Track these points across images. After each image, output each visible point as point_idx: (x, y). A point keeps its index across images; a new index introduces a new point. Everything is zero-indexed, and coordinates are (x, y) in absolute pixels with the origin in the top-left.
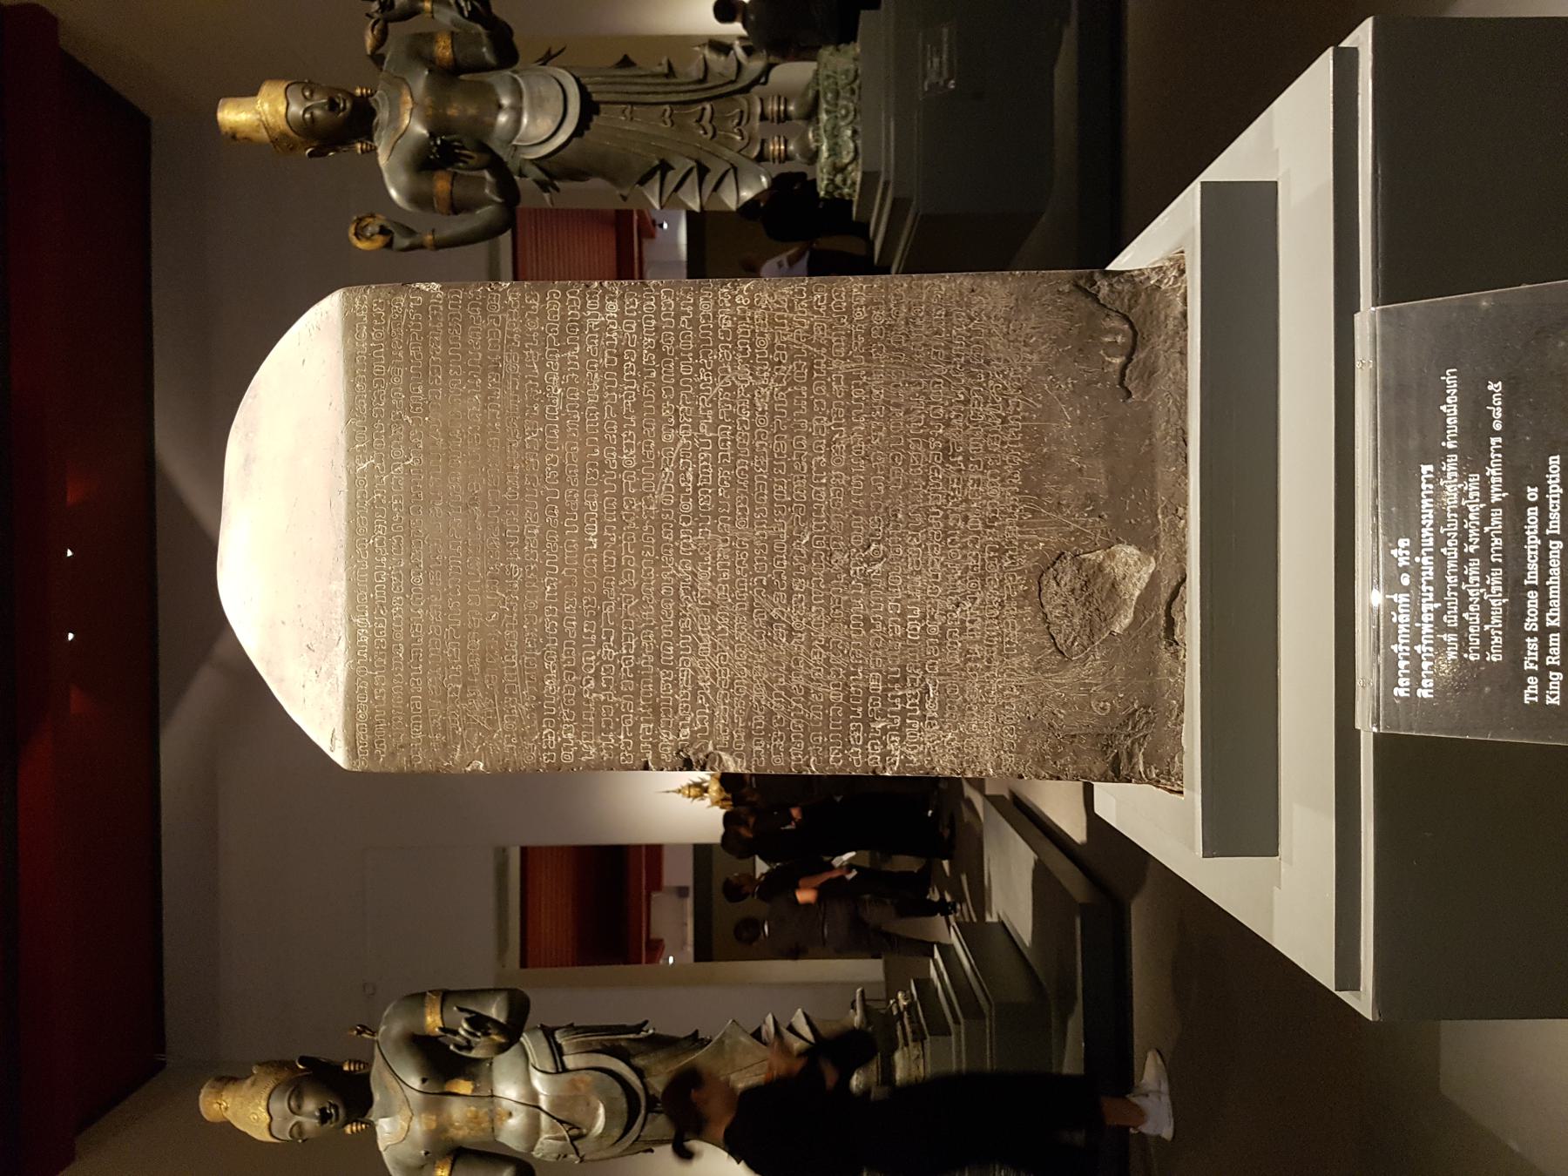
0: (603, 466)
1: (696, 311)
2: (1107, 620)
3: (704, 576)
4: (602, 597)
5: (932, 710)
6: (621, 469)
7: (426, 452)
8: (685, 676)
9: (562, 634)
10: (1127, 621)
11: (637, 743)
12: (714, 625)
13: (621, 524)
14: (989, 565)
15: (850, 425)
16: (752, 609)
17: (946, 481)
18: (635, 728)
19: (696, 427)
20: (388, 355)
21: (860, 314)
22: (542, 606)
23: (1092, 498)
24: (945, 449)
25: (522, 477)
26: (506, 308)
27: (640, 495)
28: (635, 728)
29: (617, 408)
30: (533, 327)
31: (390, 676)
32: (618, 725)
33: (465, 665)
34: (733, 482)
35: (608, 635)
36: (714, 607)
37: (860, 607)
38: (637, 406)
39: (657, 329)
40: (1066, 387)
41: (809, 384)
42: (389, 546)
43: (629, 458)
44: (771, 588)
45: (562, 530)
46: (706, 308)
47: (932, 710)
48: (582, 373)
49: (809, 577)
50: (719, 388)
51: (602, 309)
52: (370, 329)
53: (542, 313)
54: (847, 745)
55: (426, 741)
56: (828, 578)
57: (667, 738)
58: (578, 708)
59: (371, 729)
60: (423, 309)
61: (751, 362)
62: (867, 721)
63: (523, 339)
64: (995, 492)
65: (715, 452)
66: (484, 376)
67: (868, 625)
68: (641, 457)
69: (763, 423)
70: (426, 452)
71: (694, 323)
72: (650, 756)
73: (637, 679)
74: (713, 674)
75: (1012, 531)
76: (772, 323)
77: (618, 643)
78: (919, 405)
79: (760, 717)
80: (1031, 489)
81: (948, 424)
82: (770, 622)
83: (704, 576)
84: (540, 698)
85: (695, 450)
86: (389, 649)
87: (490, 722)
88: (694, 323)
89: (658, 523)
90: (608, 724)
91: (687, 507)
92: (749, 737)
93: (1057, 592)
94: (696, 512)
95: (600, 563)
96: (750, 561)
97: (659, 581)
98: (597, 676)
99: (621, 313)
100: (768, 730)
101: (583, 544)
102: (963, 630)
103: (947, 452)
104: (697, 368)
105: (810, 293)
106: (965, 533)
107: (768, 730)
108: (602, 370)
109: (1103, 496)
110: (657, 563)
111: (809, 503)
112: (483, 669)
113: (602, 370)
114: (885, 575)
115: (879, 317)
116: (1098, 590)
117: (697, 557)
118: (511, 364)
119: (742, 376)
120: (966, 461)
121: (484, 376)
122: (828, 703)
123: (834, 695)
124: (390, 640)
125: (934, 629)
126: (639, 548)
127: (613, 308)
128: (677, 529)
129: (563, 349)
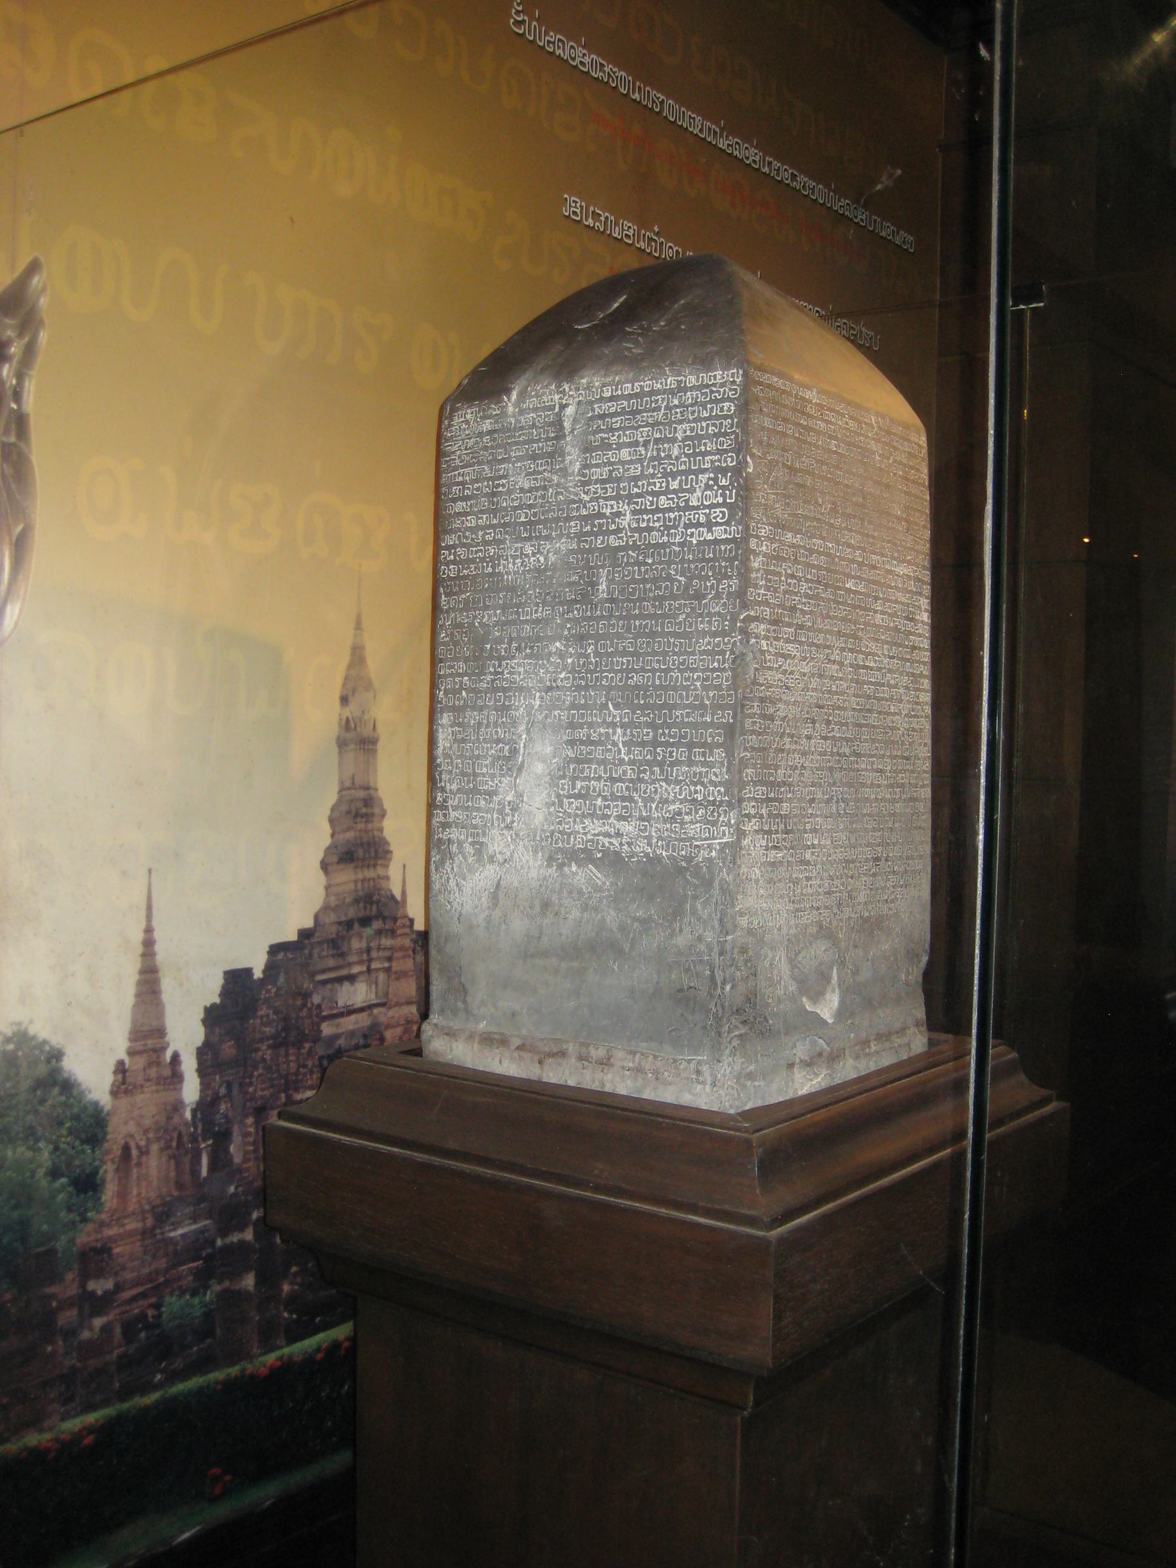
0: (876, 598)
8: (791, 648)
11: (759, 604)
12: (813, 675)
13: (855, 607)
16: (820, 707)
18: (766, 603)
22: (822, 538)
25: (873, 537)
28: (766, 603)
33: (800, 470)
34: (869, 697)
35: (810, 588)
42: (846, 429)
54: (755, 783)
55: (763, 429)
63: (917, 551)
67: (812, 800)
72: (752, 613)
74: (792, 673)
77: (807, 596)
82: (814, 722)
84: (784, 527)
86: (803, 413)
87: (772, 483)
89: (855, 637)
90: (770, 581)
92: (762, 700)
95: (840, 589)
96: (839, 708)
98: (793, 576)
100: (764, 716)
112: (798, 485)
120: (874, 875)
121: (907, 521)
122: (777, 767)
124: (809, 416)
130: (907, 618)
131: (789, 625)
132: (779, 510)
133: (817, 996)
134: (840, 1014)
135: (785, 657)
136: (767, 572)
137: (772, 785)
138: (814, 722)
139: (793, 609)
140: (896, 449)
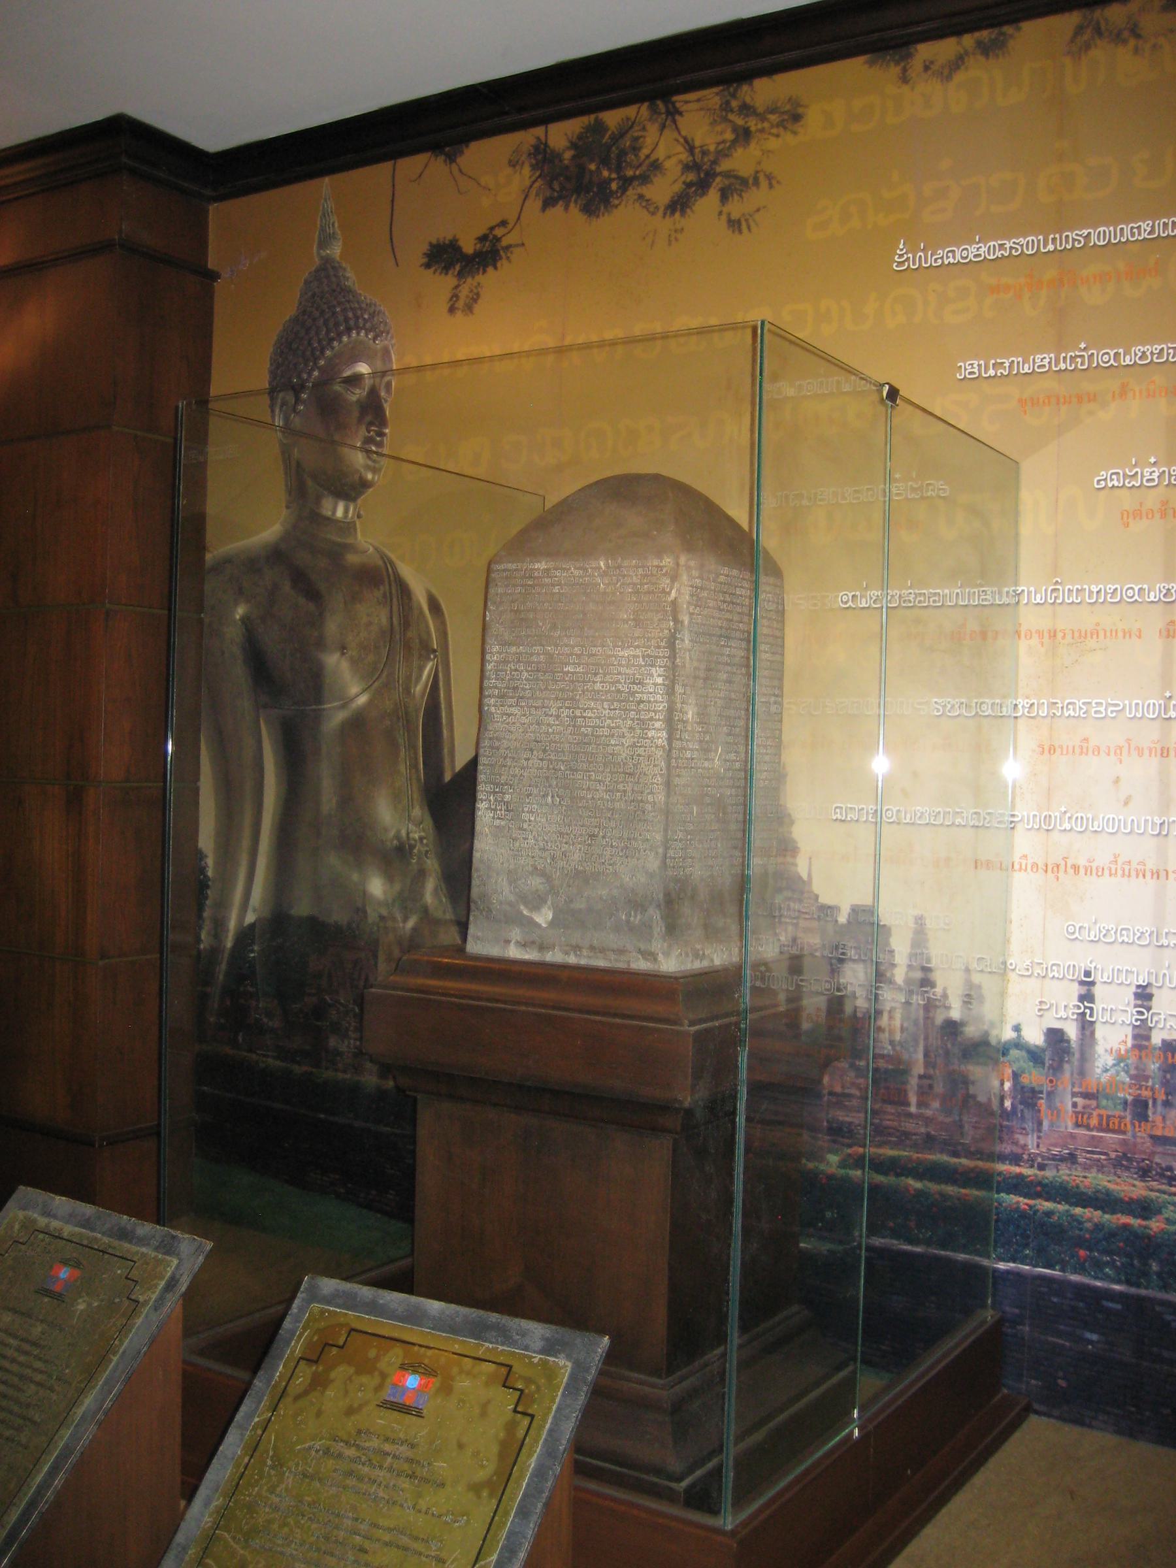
0: (596, 674)
1: (656, 720)
2: (526, 904)
3: (551, 720)
4: (545, 672)
5: (497, 822)
6: (594, 682)
7: (605, 593)
8: (515, 710)
9: (532, 654)
10: (525, 912)
13: (573, 682)
14: (547, 853)
15: (606, 791)
17: (581, 835)
18: (496, 687)
19: (609, 718)
20: (646, 575)
21: (650, 798)
23: (571, 901)
24: (594, 835)
26: (662, 630)
27: (583, 691)
28: (496, 687)
29: (618, 682)
30: (653, 642)
31: (522, 578)
32: (497, 679)
34: (586, 735)
36: (538, 724)
37: (535, 791)
38: (618, 691)
39: (649, 702)
40: (615, 892)
41: (624, 773)
43: (598, 686)
44: (545, 751)
45: (571, 654)
46: (658, 725)
47: (497, 822)
48: (633, 665)
49: (548, 768)
50: (624, 730)
51: (659, 676)
52: (657, 567)
53: (659, 647)
56: (547, 778)
57: (493, 701)
58: (506, 662)
59: (504, 570)
60: (663, 591)
61: (634, 745)
62: (495, 793)
64: (577, 857)
65: (599, 727)
66: (634, 619)
68: (599, 691)
69: (610, 750)
70: (605, 593)
71: (651, 719)
73: (514, 688)
75: (561, 864)
76: (649, 756)
78: (613, 824)
79: (497, 744)
80: (578, 873)
81: (604, 837)
82: (532, 750)
83: (551, 720)
85: (599, 718)
88: (651, 719)
89: (572, 699)
91: (578, 712)
93: (536, 883)
94: (576, 717)
96: (555, 742)
97: (549, 699)
98: (516, 670)
99: (655, 685)
101: (566, 664)
102: (525, 839)
103: (592, 836)
104: (632, 720)
105: (661, 775)
106: (561, 842)
107: (492, 748)
108: (634, 674)
109: (572, 906)
110: (557, 698)
111: (576, 770)
113: (634, 674)
114: (547, 804)
115: (649, 807)
116: (537, 902)
117: (558, 717)
118: (638, 632)
119: (627, 742)
120: (589, 845)
122: (500, 775)
123: (503, 779)
124: (535, 578)
125: (525, 826)
126: (562, 690)
127: (660, 680)
128: (569, 708)
129: (643, 657)
130: (634, 683)
131: (512, 698)
132: (507, 636)
133: (536, 908)
134: (552, 924)
135: (509, 715)
136: (497, 671)
137: (497, 785)
138: (532, 750)
139: (515, 689)
140: (624, 576)
